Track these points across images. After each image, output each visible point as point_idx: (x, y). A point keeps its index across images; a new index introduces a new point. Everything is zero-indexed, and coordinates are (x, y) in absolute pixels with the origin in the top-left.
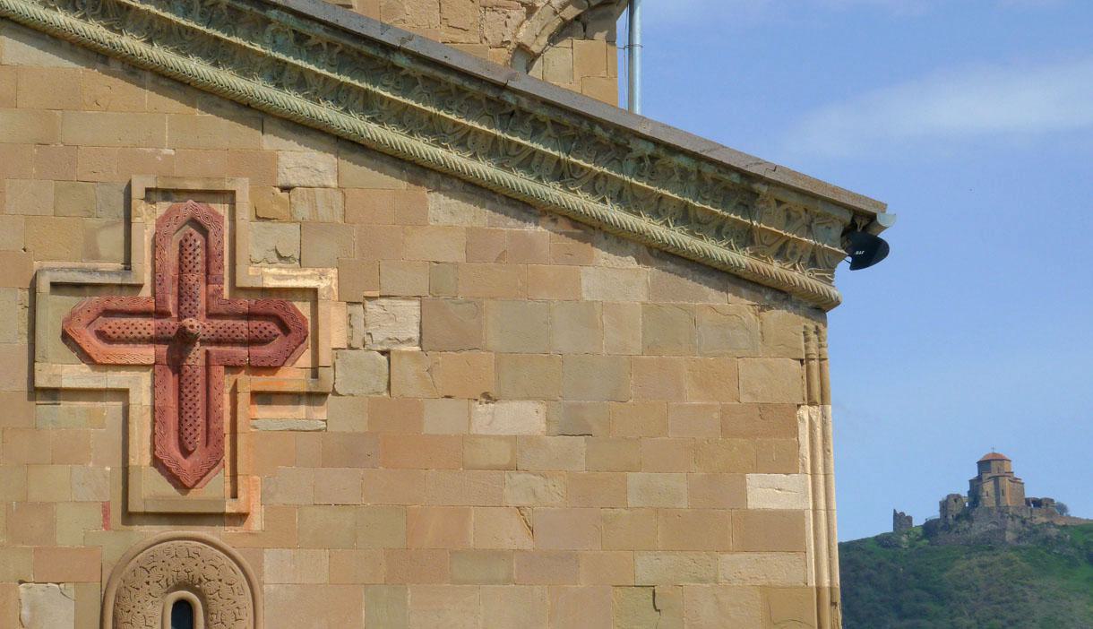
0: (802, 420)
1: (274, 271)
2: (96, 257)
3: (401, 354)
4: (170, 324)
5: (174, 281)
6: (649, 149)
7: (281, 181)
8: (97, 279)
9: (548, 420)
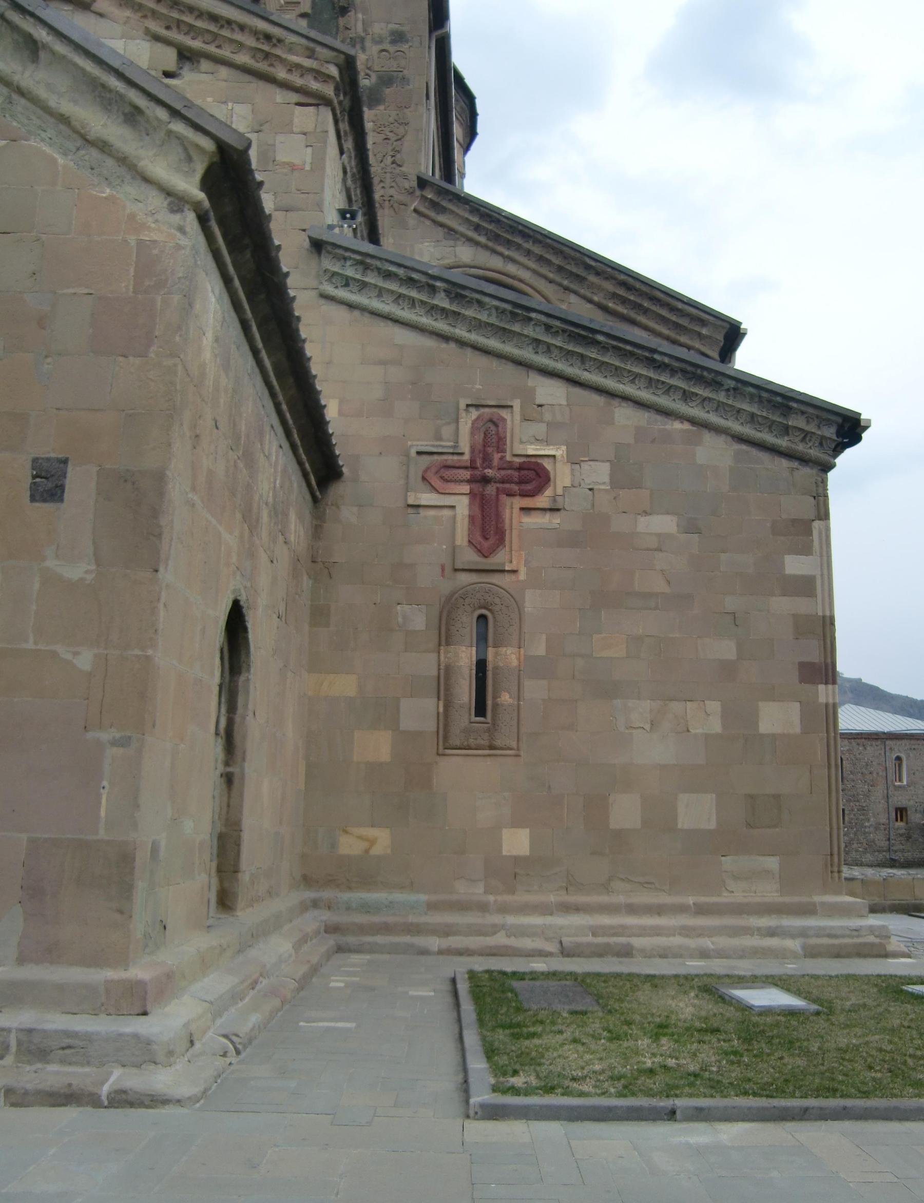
0: (815, 528)
1: (533, 447)
2: (440, 438)
3: (599, 490)
4: (477, 473)
5: (480, 452)
6: (732, 384)
7: (538, 402)
8: (440, 450)
9: (678, 526)
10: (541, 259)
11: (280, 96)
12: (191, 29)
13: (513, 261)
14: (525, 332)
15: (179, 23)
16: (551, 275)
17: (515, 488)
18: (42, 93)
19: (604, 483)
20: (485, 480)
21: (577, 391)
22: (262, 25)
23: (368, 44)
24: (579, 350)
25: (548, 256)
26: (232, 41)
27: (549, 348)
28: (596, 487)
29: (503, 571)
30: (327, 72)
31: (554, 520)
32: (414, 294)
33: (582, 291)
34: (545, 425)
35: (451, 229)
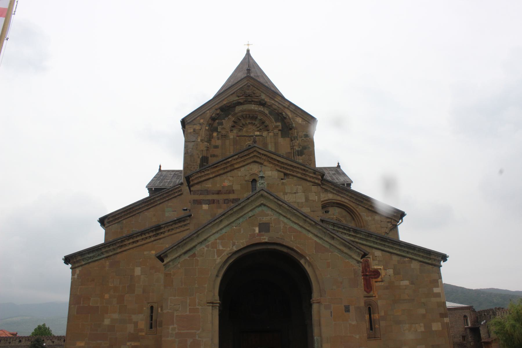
1: (376, 266)
7: (376, 255)
9: (409, 283)
10: (351, 197)
11: (308, 184)
12: (286, 169)
13: (344, 198)
14: (371, 240)
15: (283, 167)
16: (354, 201)
17: (373, 276)
18: (335, 244)
19: (392, 274)
20: (367, 275)
21: (384, 252)
22: (303, 167)
23: (298, 138)
24: (383, 243)
25: (353, 196)
26: (296, 171)
27: (377, 243)
28: (391, 275)
29: (373, 296)
30: (319, 178)
31: (383, 284)
32: (345, 232)
33: (362, 205)
34: (377, 261)
35: (326, 189)
